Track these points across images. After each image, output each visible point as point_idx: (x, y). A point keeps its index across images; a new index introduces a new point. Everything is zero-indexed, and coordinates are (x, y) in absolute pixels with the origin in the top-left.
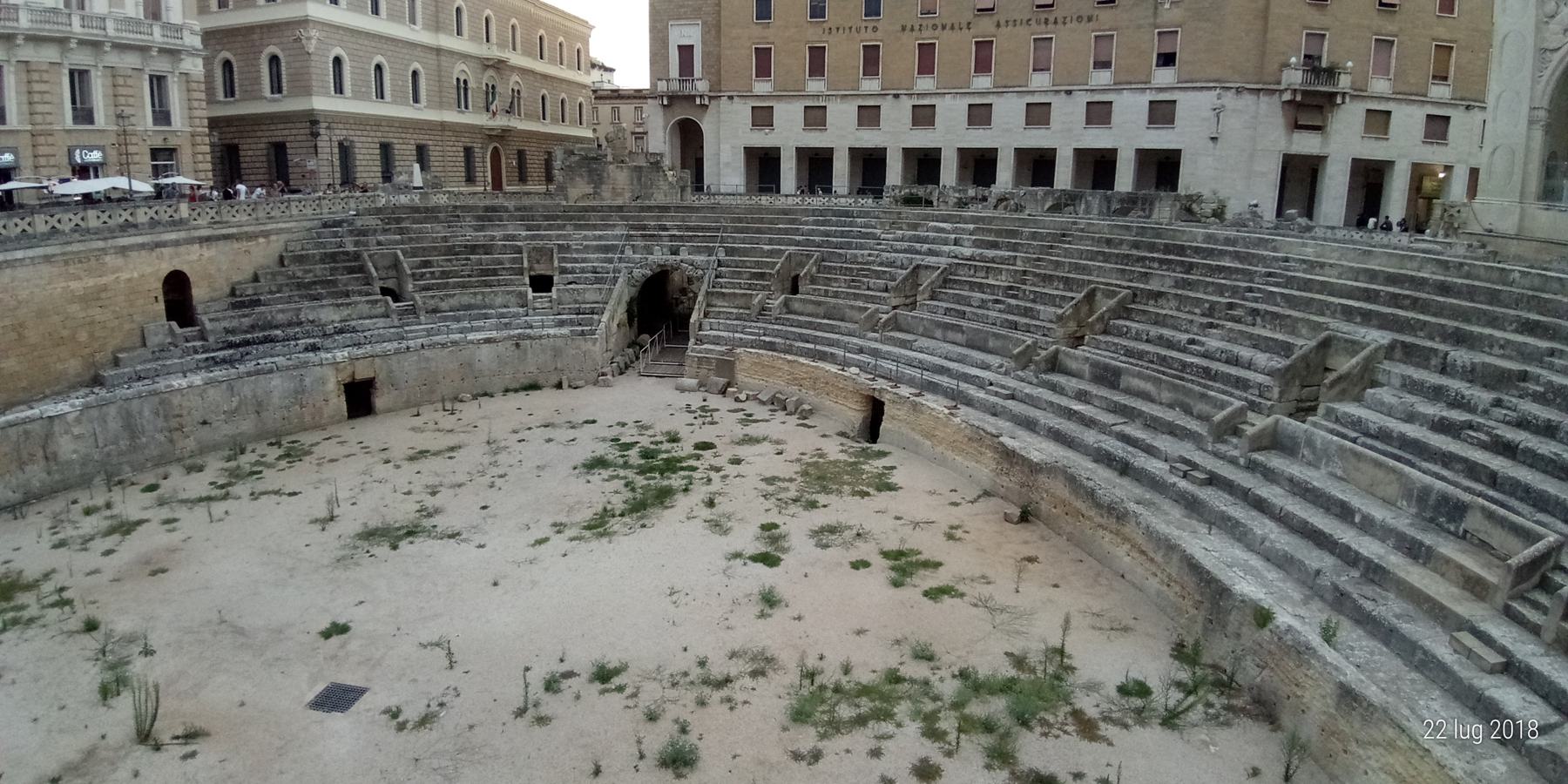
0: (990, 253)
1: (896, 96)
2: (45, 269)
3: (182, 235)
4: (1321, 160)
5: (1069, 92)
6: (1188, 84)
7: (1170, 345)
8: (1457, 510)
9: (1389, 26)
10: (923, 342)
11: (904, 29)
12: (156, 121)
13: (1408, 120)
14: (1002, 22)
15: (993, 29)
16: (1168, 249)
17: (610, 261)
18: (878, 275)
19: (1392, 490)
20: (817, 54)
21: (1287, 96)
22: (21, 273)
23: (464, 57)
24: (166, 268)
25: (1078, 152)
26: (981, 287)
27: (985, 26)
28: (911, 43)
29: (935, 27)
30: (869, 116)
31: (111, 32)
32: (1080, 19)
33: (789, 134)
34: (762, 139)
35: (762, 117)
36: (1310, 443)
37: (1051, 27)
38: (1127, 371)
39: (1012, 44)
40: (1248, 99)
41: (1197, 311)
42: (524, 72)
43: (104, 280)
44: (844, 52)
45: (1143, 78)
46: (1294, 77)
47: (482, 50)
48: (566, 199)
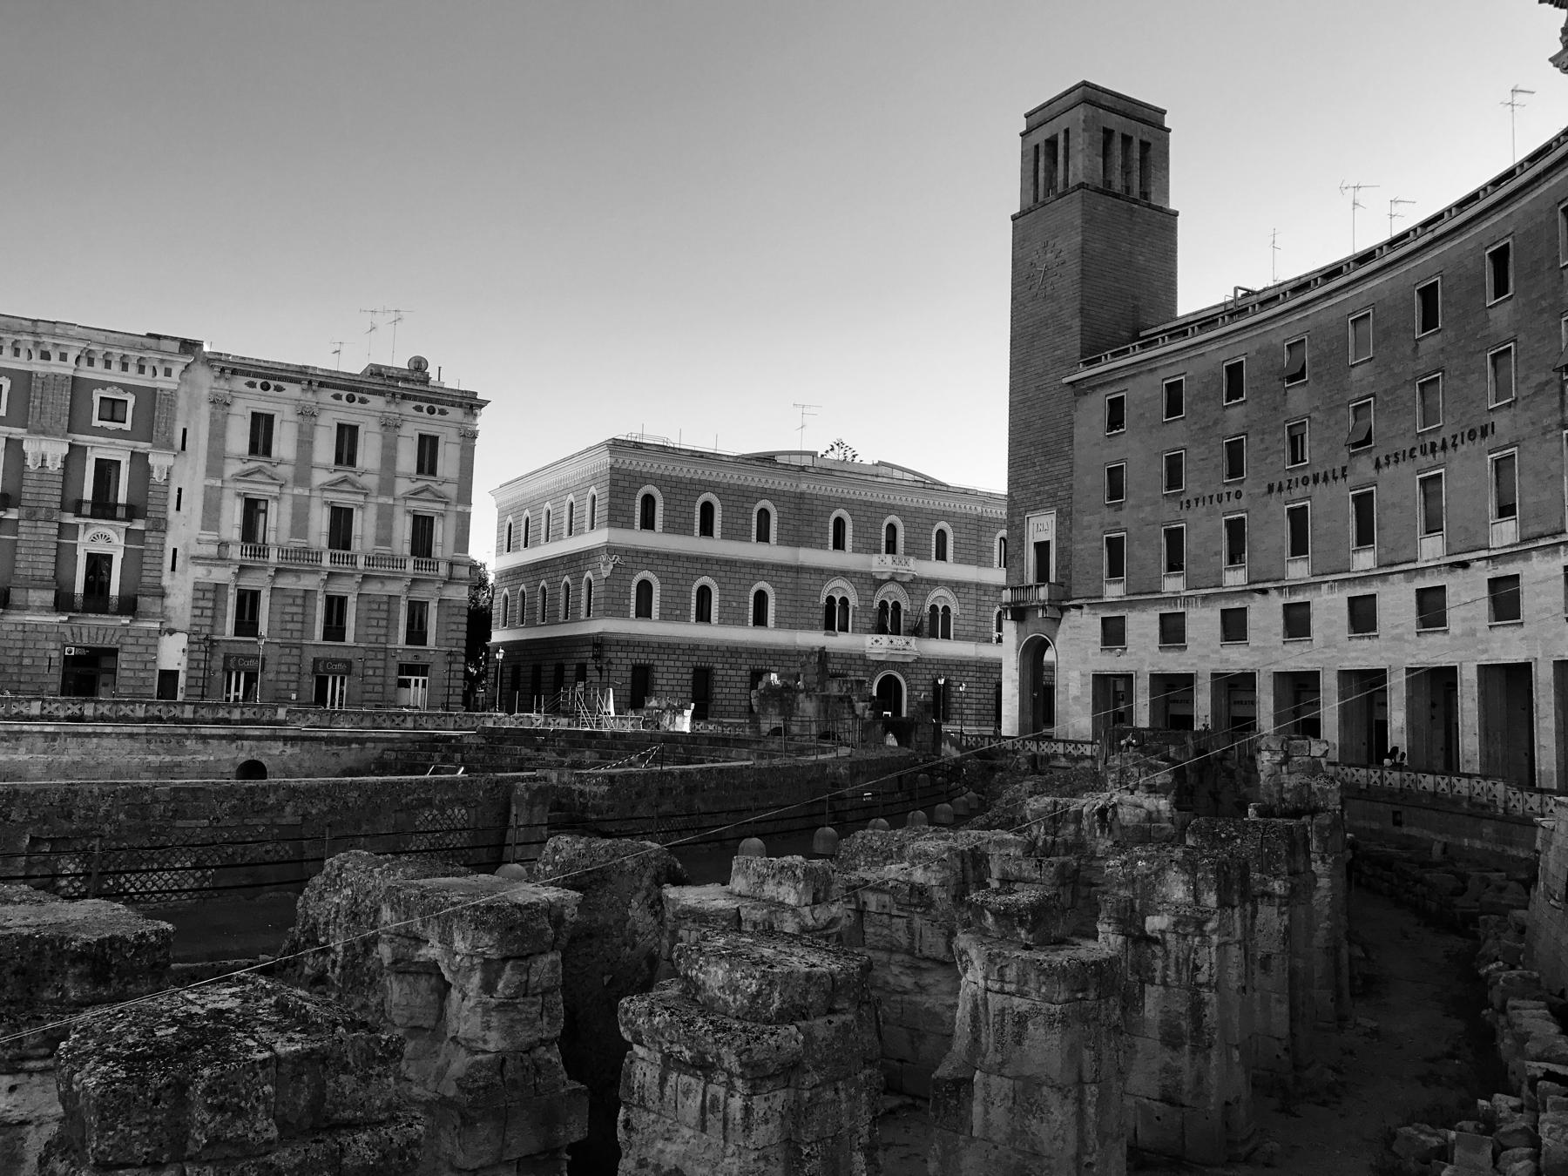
1: (1264, 592)
2: (127, 742)
3: (267, 733)
5: (1465, 565)
11: (1271, 488)
12: (410, 640)
14: (1383, 460)
15: (1372, 473)
20: (1175, 538)
22: (106, 742)
23: (844, 574)
24: (243, 757)
25: (1484, 670)
27: (1364, 467)
28: (1280, 509)
29: (1305, 481)
31: (361, 565)
32: (1472, 435)
33: (1143, 654)
34: (1112, 663)
35: (1113, 634)
37: (1439, 455)
39: (1398, 489)
42: (956, 586)
43: (179, 759)
44: (1205, 532)
45: (1556, 525)
47: (881, 564)
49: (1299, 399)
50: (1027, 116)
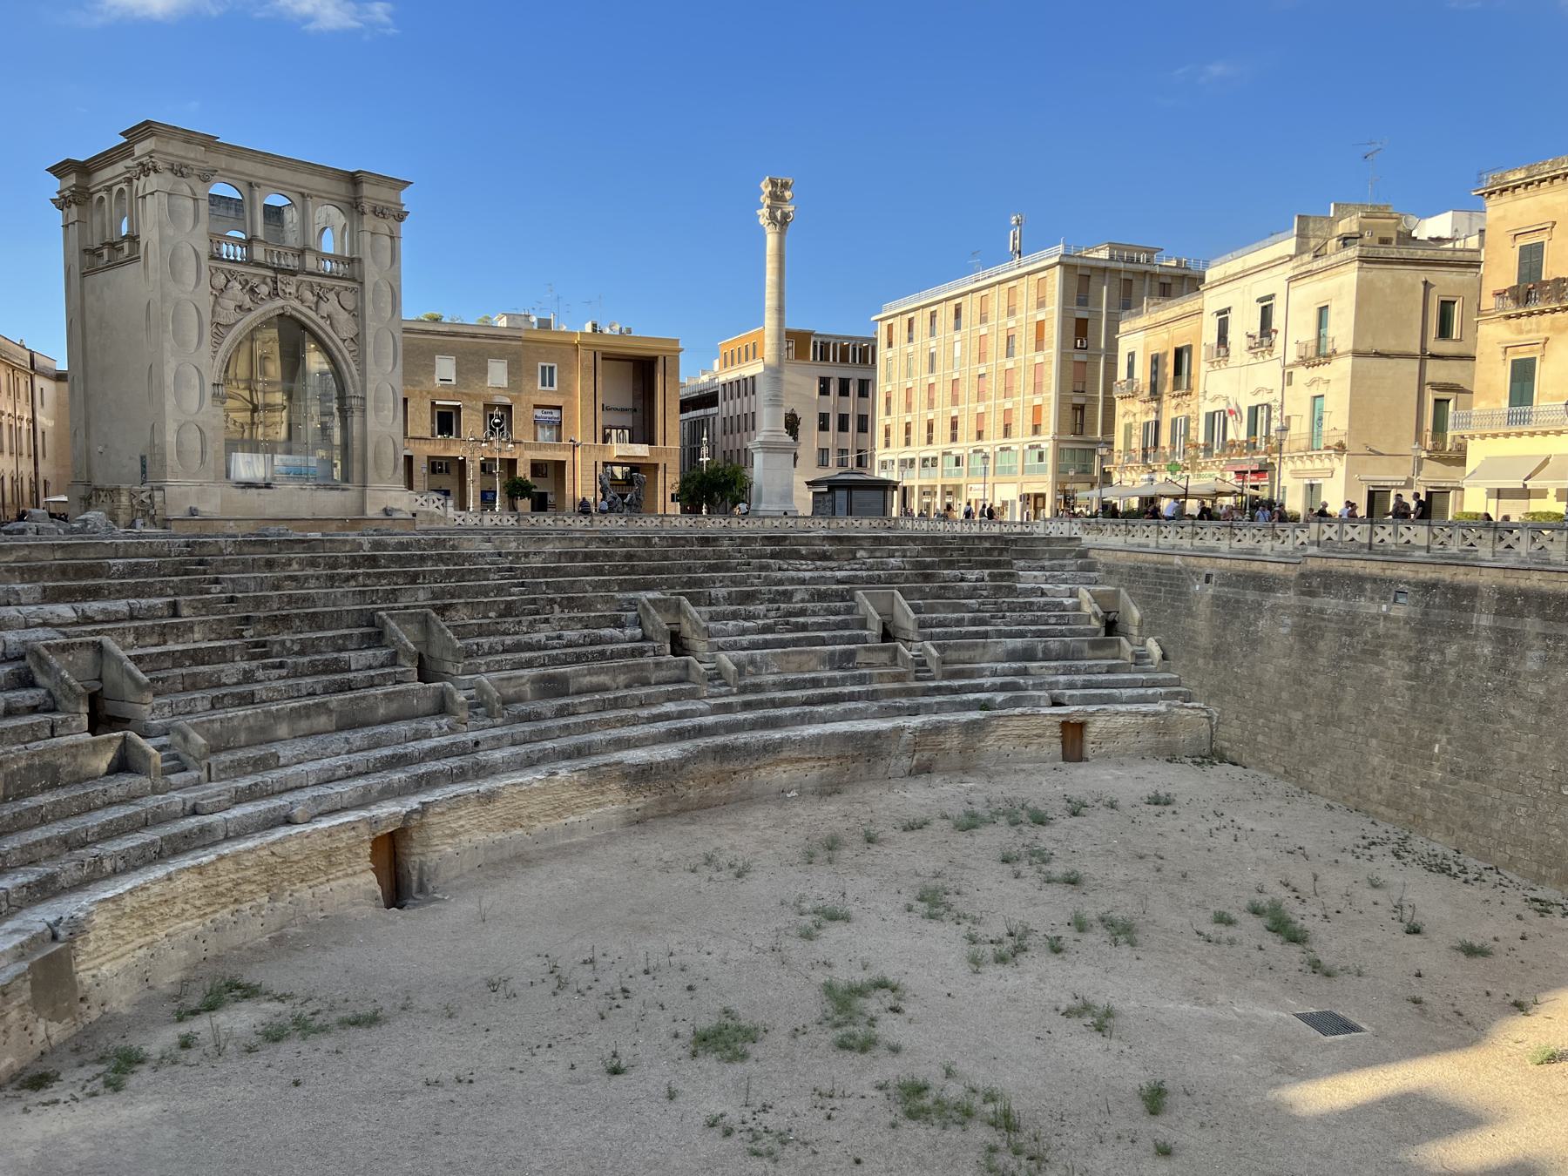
7: (530, 647)
8: (849, 656)
19: (814, 663)
36: (752, 662)
38: (577, 675)
41: (492, 614)
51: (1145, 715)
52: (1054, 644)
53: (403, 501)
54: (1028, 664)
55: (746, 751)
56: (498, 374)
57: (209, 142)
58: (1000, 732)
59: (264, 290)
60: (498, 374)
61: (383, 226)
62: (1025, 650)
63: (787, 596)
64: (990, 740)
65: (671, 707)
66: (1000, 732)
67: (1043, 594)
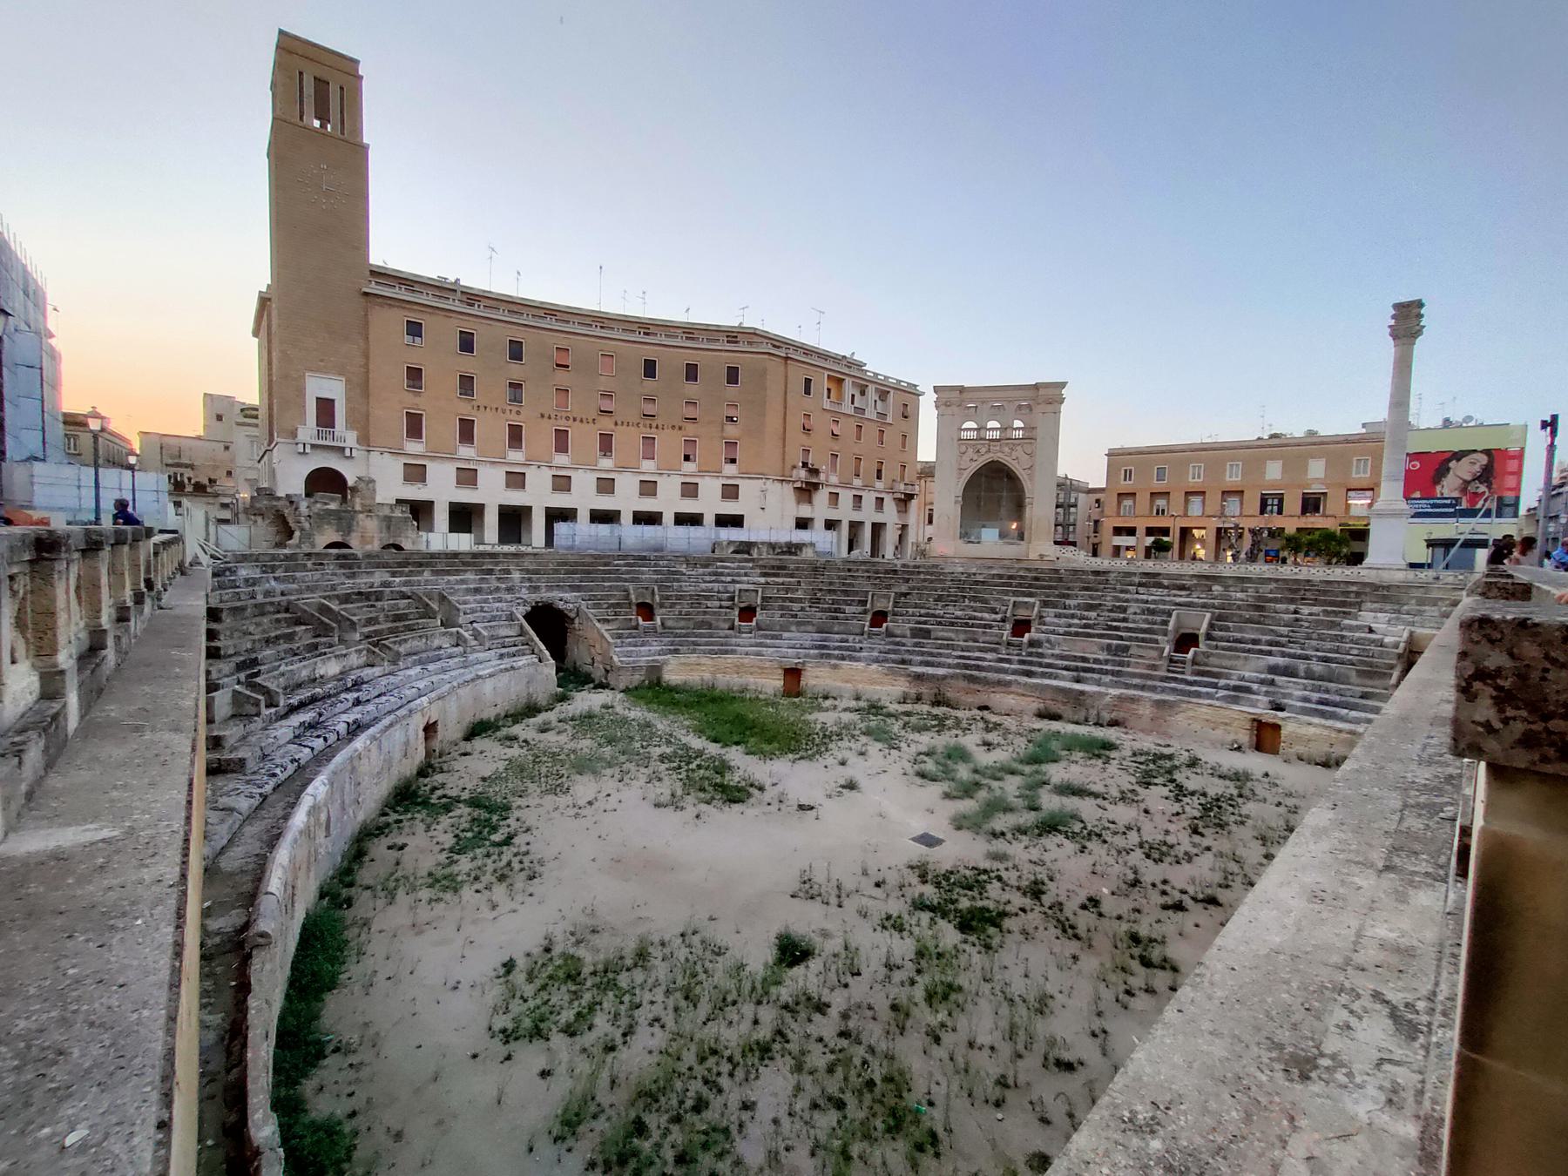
0: (780, 580)
4: (812, 519)
6: (747, 475)
9: (836, 447)
10: (786, 635)
13: (846, 497)
16: (887, 572)
17: (486, 601)
18: (707, 598)
19: (1095, 648)
21: (798, 485)
26: (792, 600)
27: (606, 424)
28: (549, 428)
30: (516, 480)
36: (1048, 641)
40: (778, 485)
46: (803, 474)
48: (313, 546)
49: (562, 377)
50: (281, 32)
51: (1340, 731)
52: (1318, 667)
53: (1052, 551)
54: (1277, 678)
55: (986, 682)
56: (1316, 469)
57: (962, 389)
58: (1191, 714)
59: (983, 450)
60: (1316, 469)
61: (1050, 408)
62: (1286, 667)
63: (1124, 610)
64: (1180, 717)
65: (977, 654)
66: (1191, 714)
67: (1371, 631)
